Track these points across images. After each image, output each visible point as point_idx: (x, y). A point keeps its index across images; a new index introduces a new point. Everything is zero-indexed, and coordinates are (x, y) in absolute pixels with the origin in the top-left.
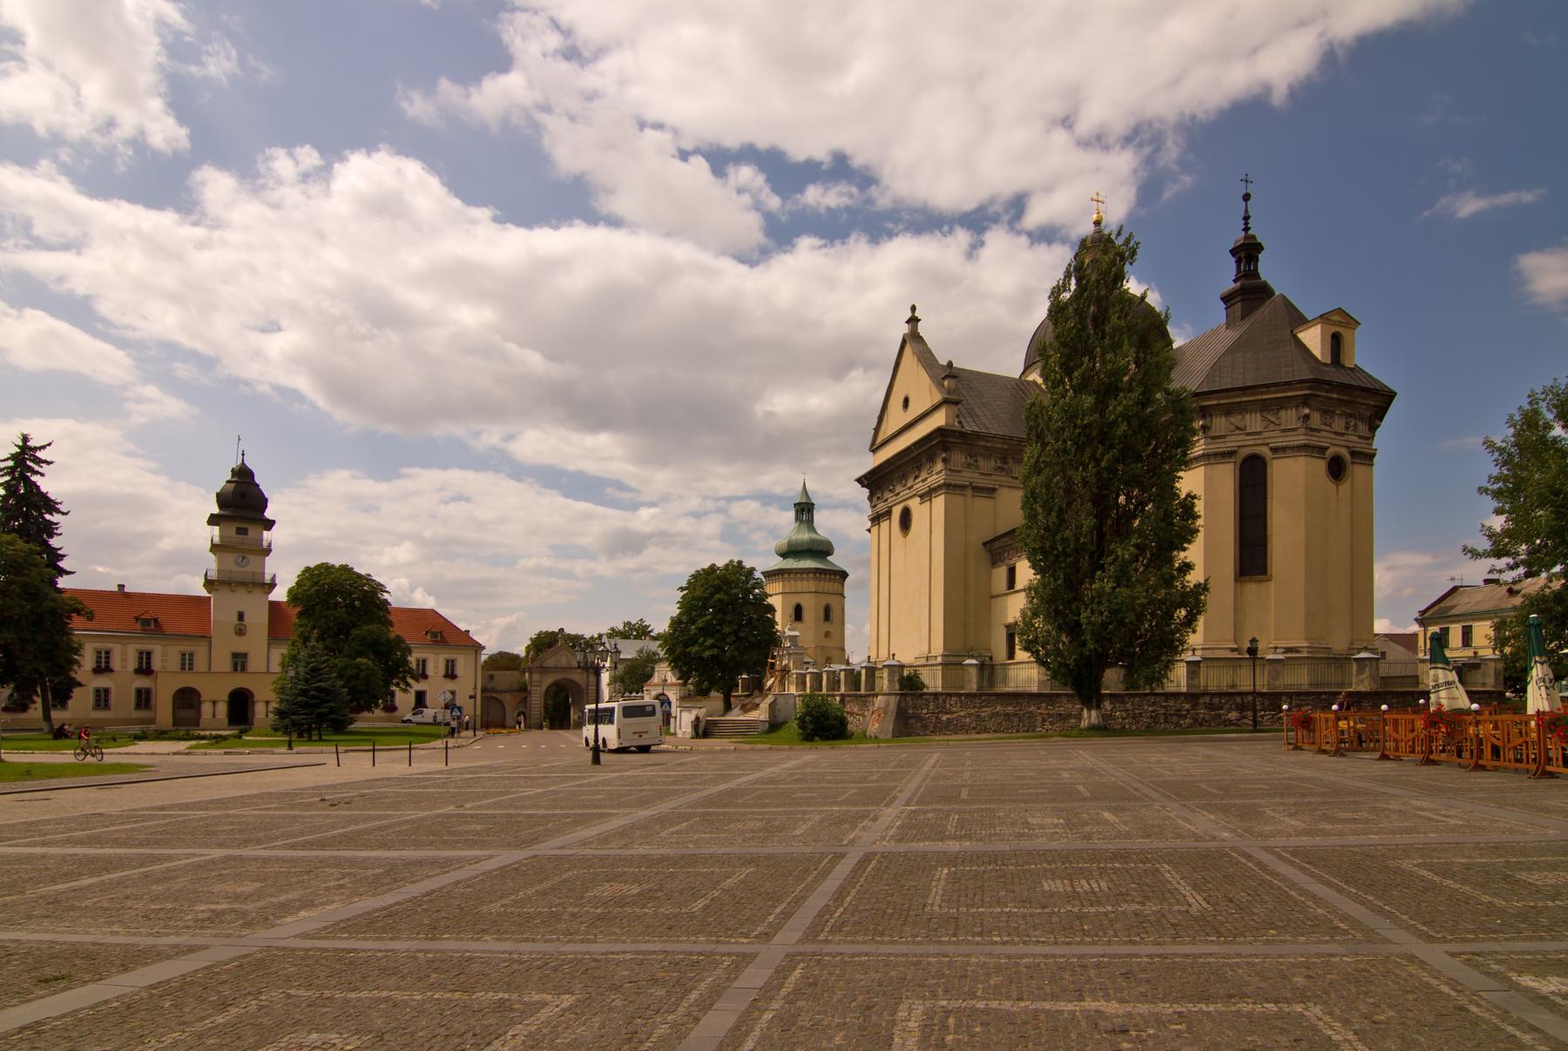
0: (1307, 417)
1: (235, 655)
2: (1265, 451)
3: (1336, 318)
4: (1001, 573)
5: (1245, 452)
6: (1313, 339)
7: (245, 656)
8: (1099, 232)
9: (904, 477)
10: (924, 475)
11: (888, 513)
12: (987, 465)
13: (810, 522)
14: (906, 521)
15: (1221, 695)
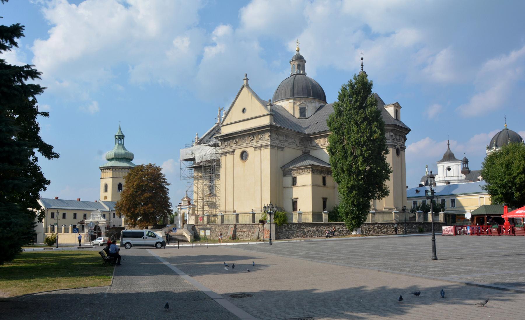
0: (392, 136)
3: (396, 105)
4: (288, 180)
6: (390, 110)
10: (256, 139)
11: (233, 152)
12: (281, 138)
13: (122, 145)
14: (244, 156)
15: (381, 224)
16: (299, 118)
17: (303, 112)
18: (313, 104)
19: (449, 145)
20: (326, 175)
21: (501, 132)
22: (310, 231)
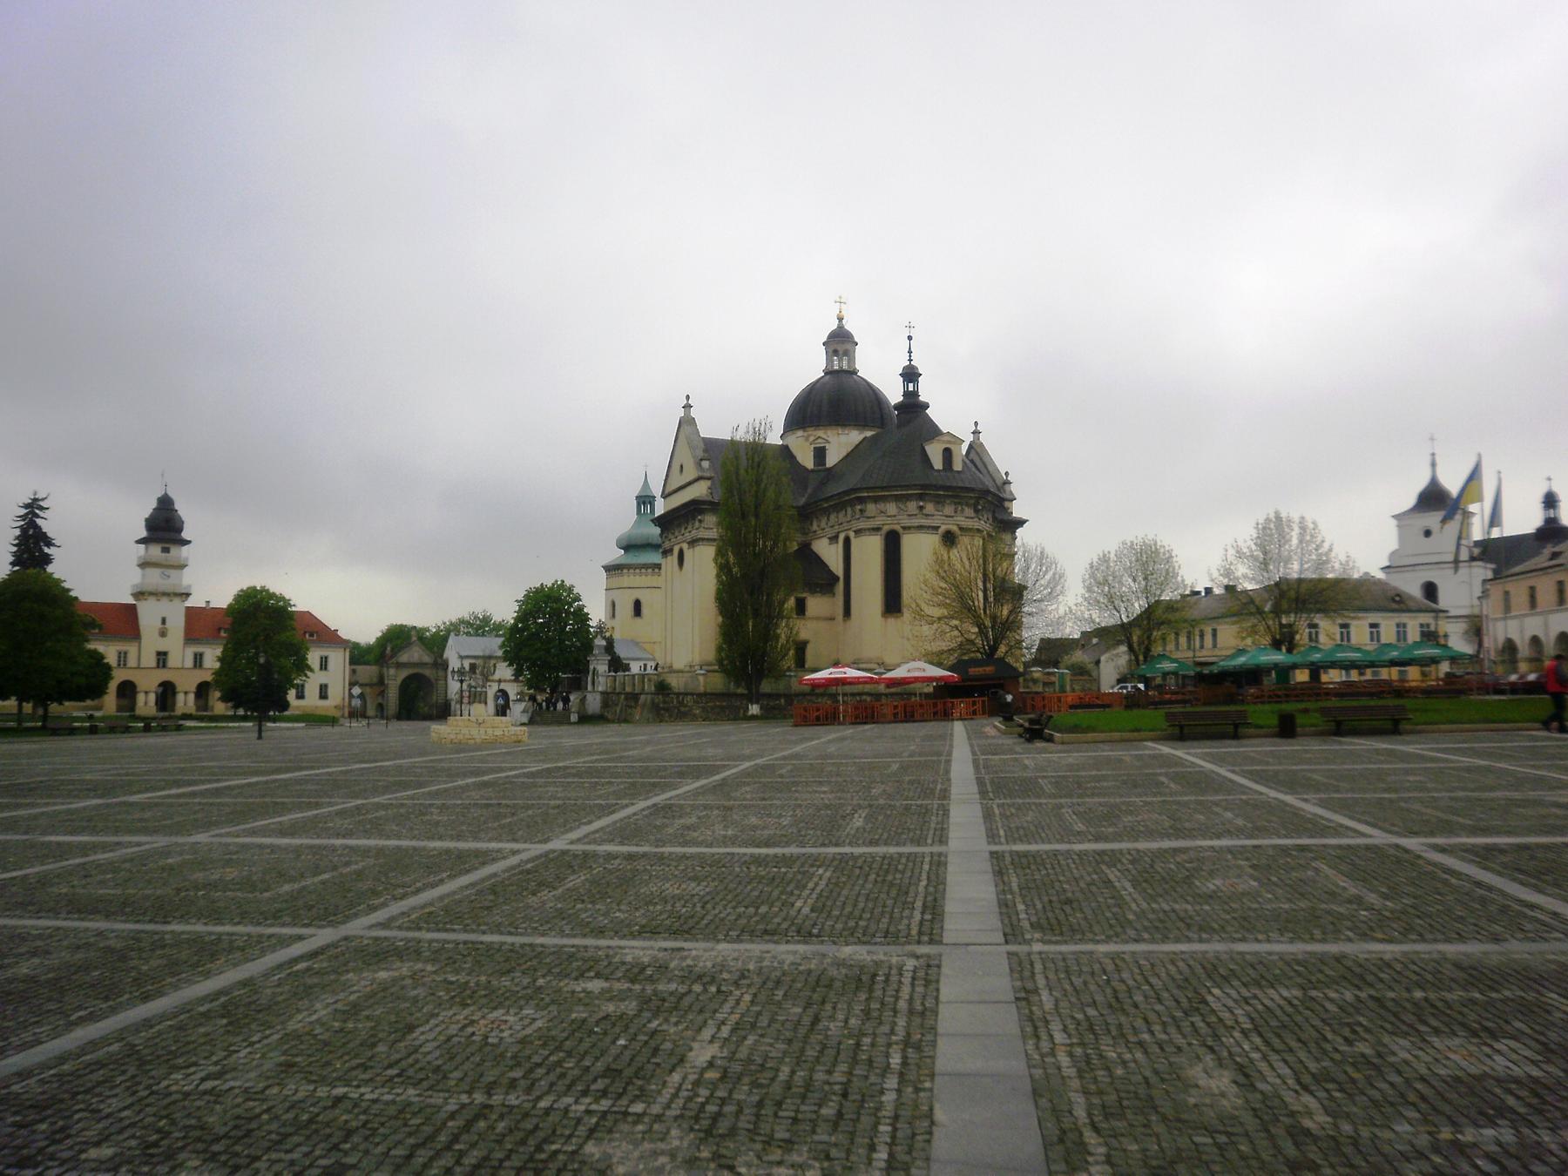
1: (159, 654)
2: (897, 528)
5: (886, 528)
7: (165, 654)
8: (841, 327)
9: (679, 526)
11: (671, 550)
17: (820, 454)
18: (843, 438)
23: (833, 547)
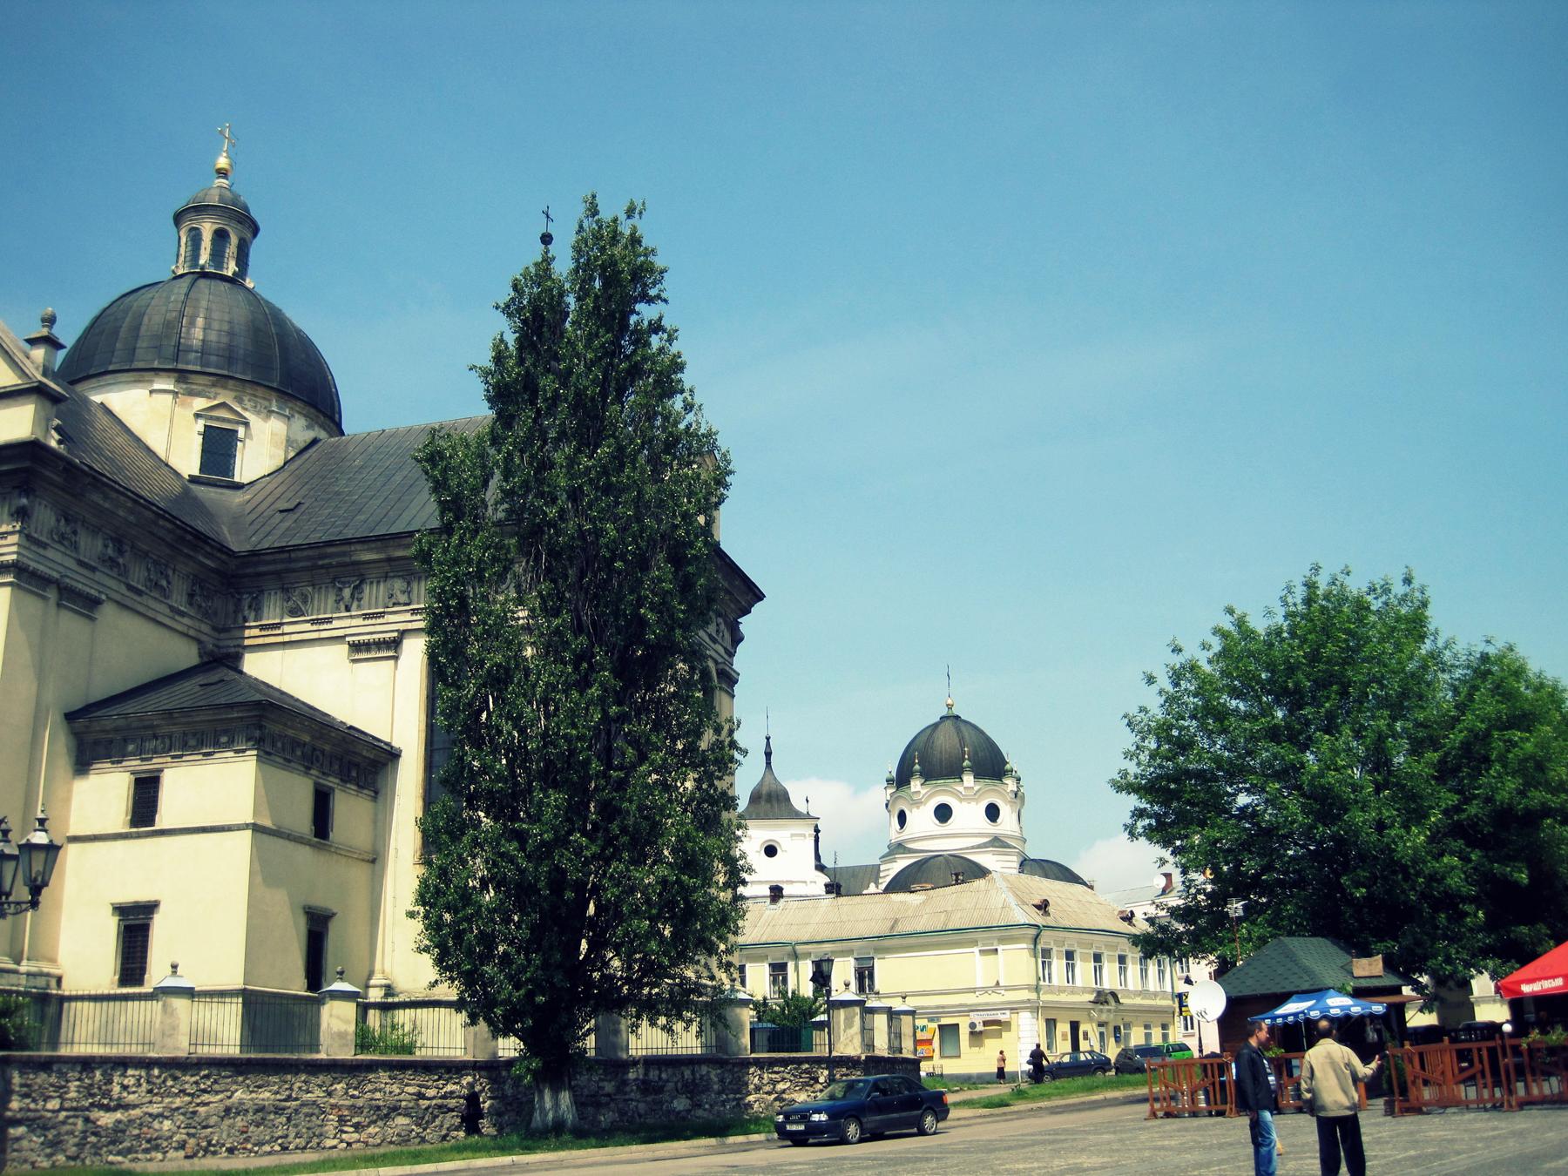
12: (91, 546)
16: (193, 480)
17: (219, 447)
19: (768, 754)
20: (332, 782)
21: (935, 726)
22: (240, 1110)
23: (376, 671)
